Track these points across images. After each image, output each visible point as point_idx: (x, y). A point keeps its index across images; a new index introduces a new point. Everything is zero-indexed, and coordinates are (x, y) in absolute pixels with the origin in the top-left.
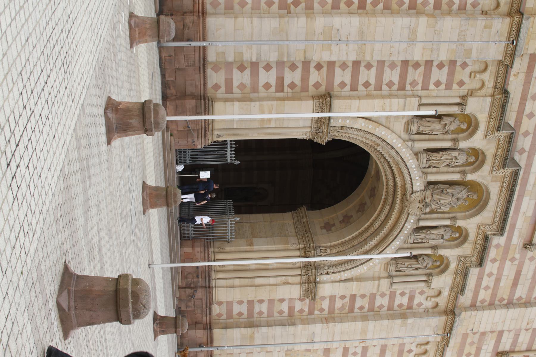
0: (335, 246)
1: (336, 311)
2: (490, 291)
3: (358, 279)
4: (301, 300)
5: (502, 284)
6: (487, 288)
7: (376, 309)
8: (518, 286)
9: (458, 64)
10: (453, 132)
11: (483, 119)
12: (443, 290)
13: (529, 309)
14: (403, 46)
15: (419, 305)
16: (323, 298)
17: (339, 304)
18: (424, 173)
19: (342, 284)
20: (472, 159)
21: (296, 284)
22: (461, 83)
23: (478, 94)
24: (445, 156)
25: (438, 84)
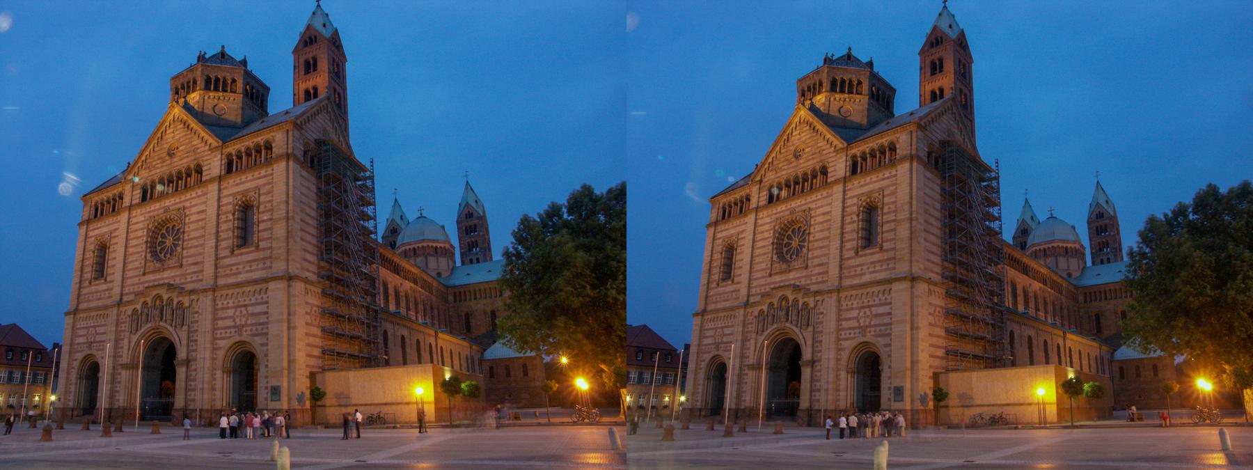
5: (196, 270)
6: (198, 276)
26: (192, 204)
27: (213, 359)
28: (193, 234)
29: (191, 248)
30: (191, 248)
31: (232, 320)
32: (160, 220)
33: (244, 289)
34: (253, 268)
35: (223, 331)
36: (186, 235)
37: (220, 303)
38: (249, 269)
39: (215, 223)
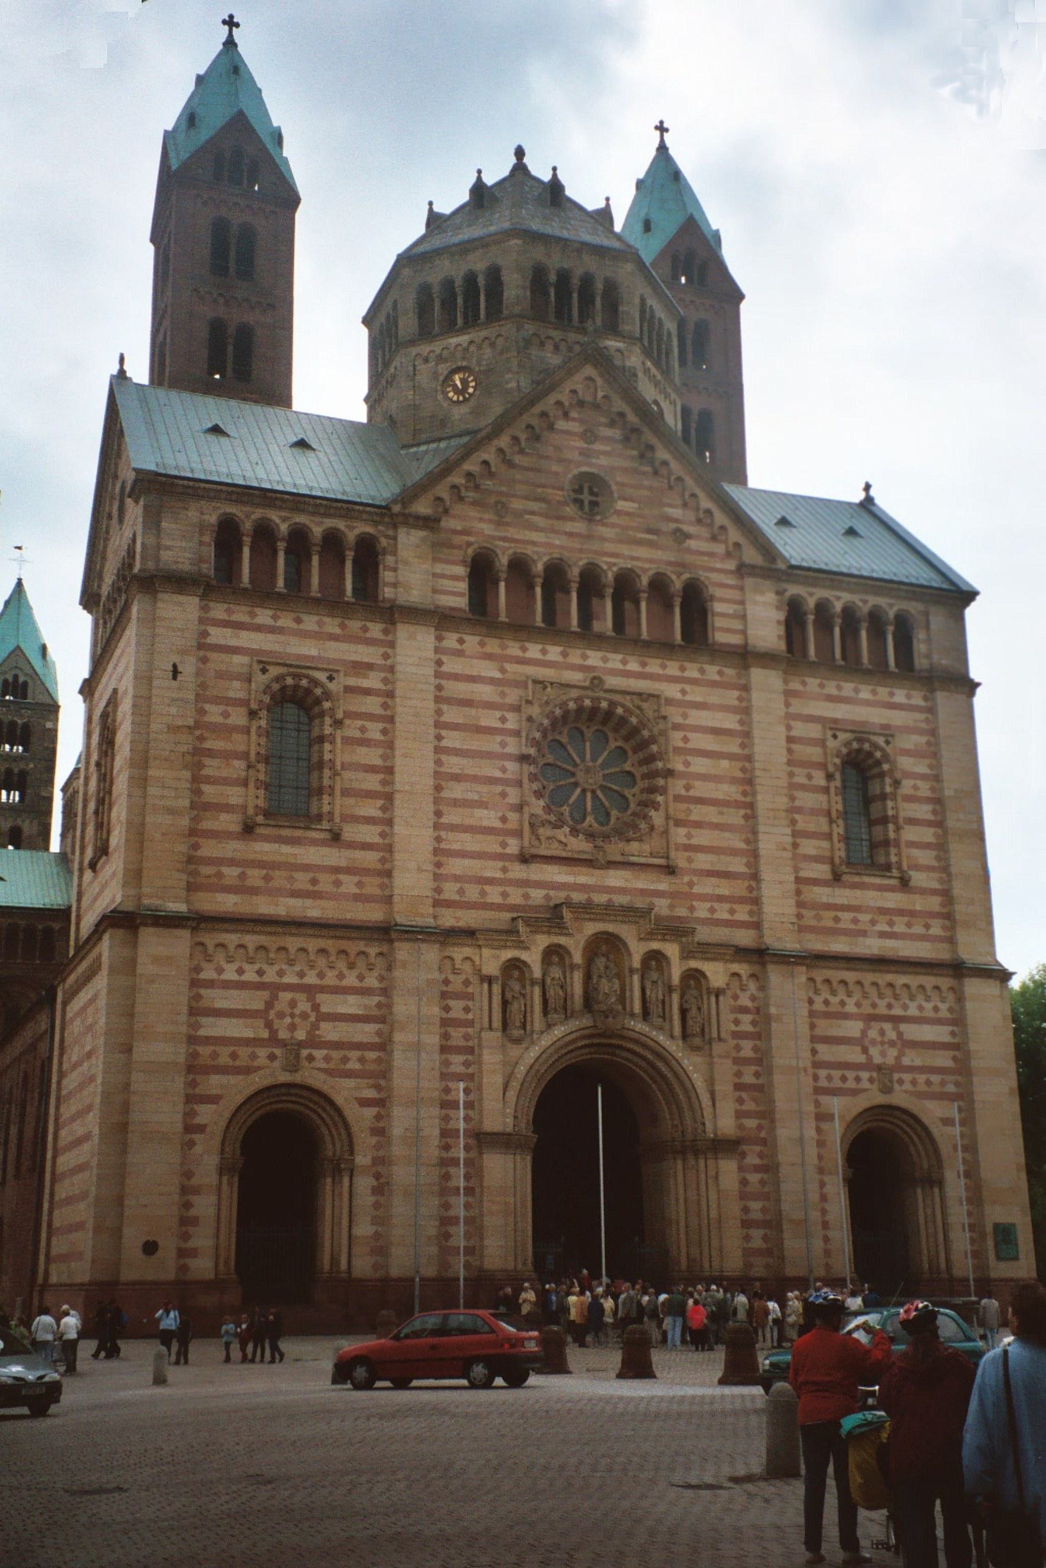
0: (671, 1114)
1: (762, 1108)
2: (736, 906)
3: (711, 1082)
4: (743, 1155)
5: (727, 892)
6: (732, 912)
7: (759, 1055)
8: (731, 869)
9: (445, 989)
10: (524, 987)
11: (508, 954)
12: (732, 971)
13: (762, 852)
14: (423, 1055)
15: (753, 998)
16: (741, 1127)
17: (750, 1106)
18: (572, 1016)
19: (717, 1104)
20: (555, 959)
21: (717, 1164)
22: (467, 983)
23: (478, 963)
24: (551, 993)
25: (467, 1010)
26: (688, 698)
27: (821, 1144)
28: (700, 789)
29: (698, 825)
30: (698, 825)
31: (859, 1049)
32: (572, 705)
33: (890, 977)
34: (900, 928)
35: (836, 1074)
36: (681, 783)
37: (818, 1000)
38: (887, 929)
39: (783, 782)
